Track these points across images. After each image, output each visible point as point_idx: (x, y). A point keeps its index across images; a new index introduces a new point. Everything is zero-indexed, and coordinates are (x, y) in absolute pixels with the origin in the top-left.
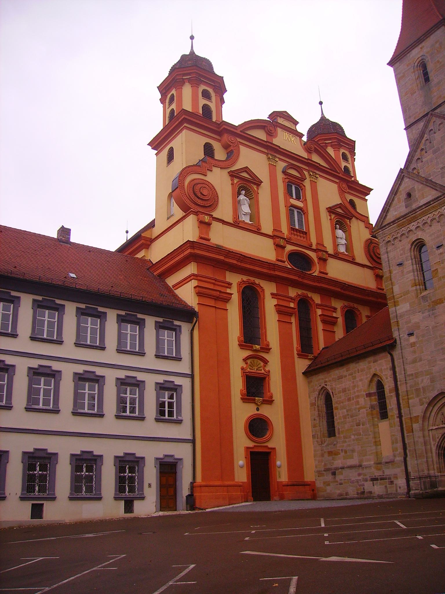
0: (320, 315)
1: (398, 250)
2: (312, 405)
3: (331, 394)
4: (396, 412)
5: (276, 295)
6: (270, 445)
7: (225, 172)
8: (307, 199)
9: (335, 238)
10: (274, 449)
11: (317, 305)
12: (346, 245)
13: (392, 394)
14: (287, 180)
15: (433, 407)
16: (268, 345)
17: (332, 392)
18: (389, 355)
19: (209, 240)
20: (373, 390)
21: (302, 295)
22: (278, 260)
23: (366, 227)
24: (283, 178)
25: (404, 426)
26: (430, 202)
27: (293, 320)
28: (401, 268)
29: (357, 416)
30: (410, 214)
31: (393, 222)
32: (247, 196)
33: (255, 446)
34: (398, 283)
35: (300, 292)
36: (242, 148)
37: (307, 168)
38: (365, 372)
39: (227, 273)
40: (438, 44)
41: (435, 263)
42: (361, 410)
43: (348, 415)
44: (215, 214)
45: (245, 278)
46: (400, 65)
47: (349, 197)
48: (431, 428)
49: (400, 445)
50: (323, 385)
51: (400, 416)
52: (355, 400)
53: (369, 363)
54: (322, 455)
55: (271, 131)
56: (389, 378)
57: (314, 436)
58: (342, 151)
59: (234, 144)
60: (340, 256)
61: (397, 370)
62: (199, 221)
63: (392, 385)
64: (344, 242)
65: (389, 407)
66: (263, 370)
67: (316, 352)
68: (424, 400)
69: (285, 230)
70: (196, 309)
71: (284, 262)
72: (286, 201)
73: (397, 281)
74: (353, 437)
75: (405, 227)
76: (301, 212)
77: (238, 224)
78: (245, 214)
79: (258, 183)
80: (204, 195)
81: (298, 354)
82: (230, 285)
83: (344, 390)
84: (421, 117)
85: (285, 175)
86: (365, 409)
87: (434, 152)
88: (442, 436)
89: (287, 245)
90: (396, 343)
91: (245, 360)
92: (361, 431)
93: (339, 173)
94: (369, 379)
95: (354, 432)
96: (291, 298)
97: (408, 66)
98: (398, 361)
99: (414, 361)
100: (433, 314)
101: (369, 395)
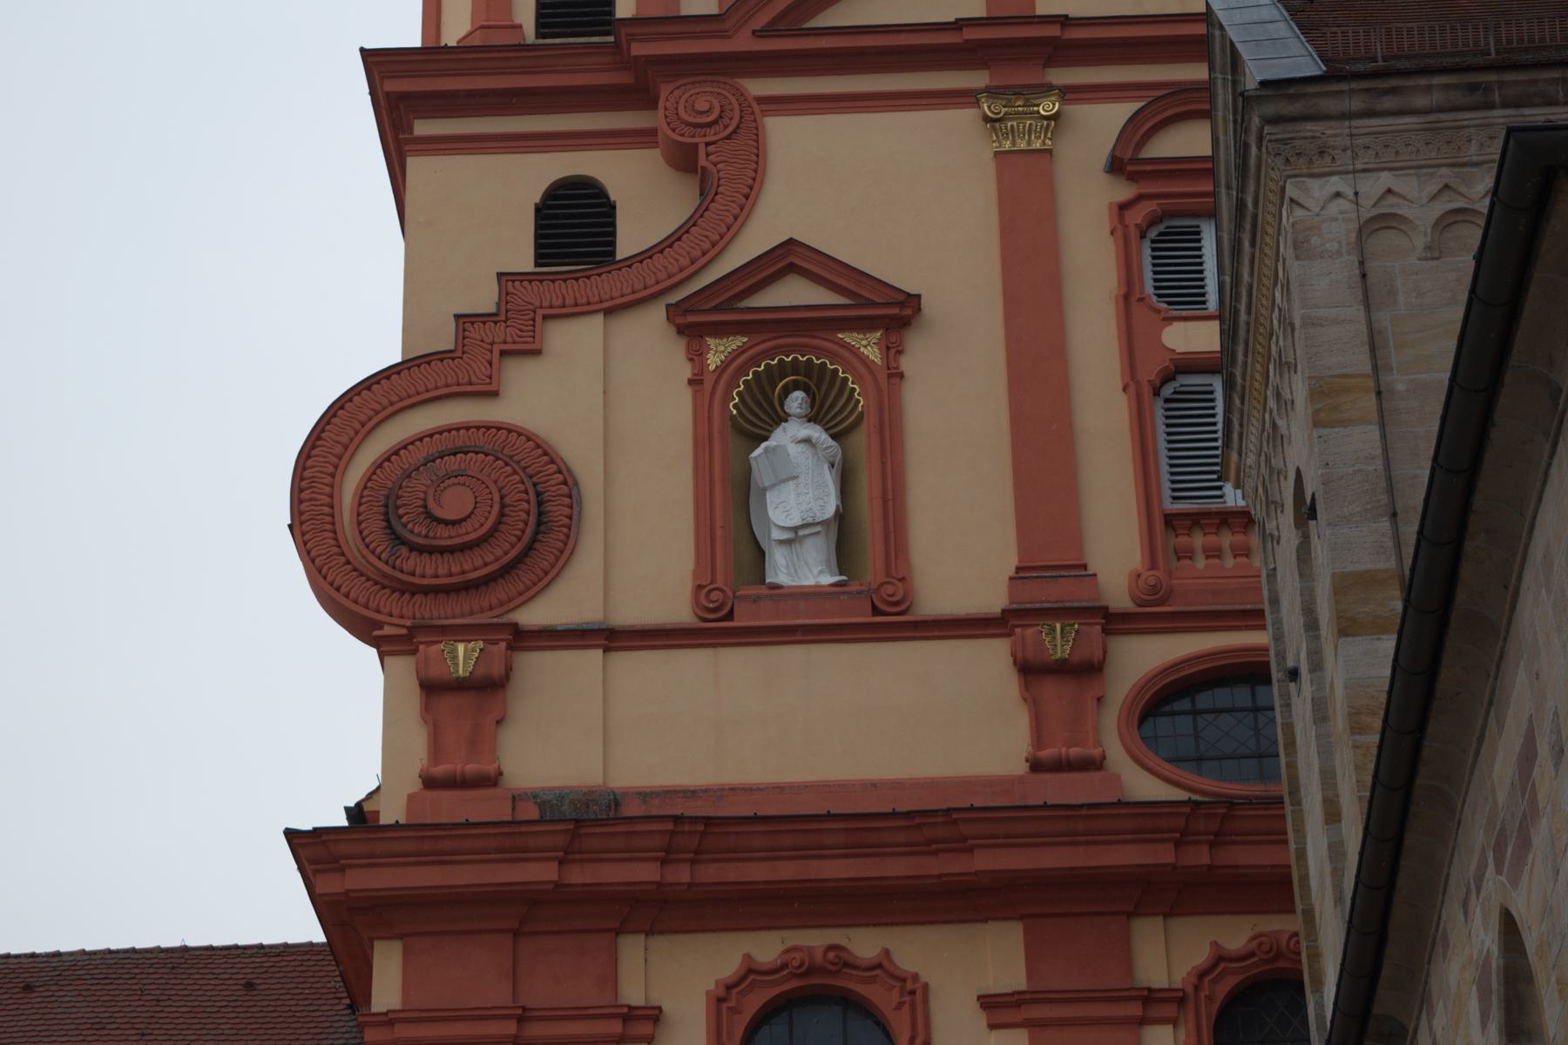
19: (491, 781)
32: (823, 418)
39: (632, 950)
45: (767, 947)
59: (726, 121)
80: (459, 522)
85: (1132, 177)
96: (1150, 997)
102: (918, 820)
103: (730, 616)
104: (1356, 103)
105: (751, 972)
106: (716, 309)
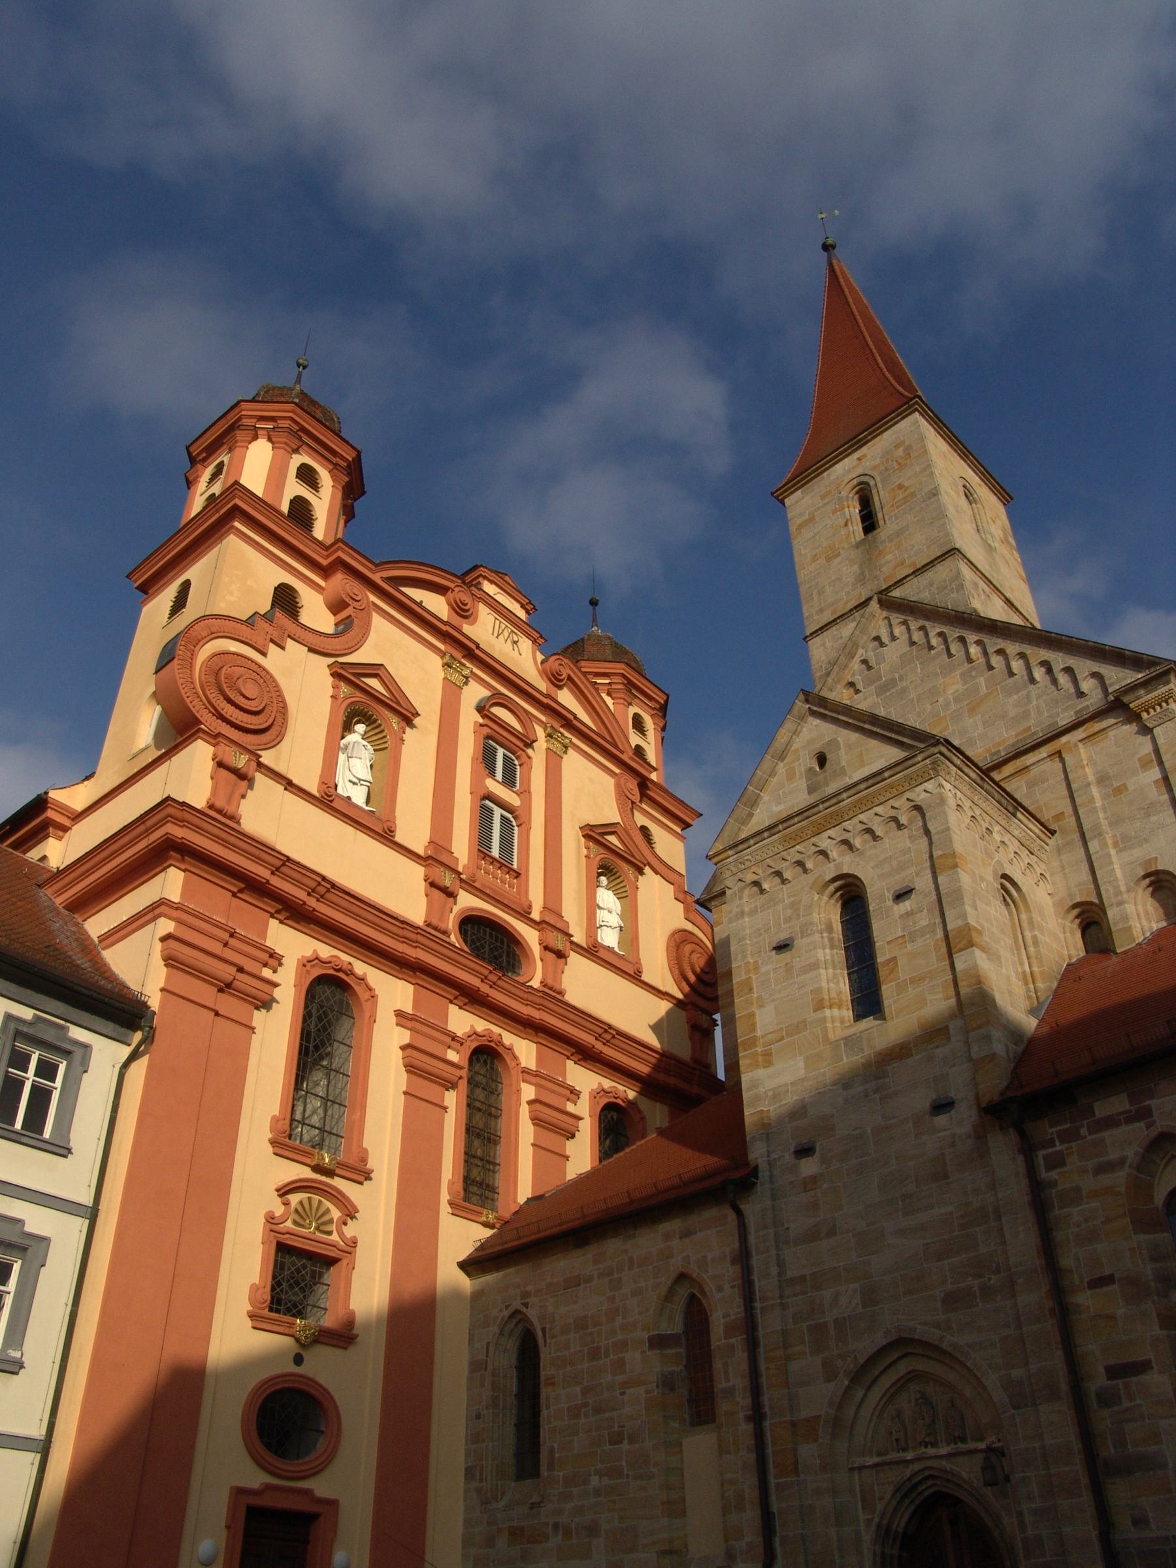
0: (530, 1103)
1: (781, 906)
2: (477, 1366)
3: (539, 1333)
4: (743, 1401)
5: (411, 1020)
6: (321, 1487)
7: (321, 665)
8: (532, 790)
9: (592, 907)
10: (333, 1503)
11: (525, 1071)
12: (621, 930)
13: (733, 1340)
14: (486, 731)
15: (868, 1389)
16: (364, 1160)
17: (544, 1330)
18: (732, 1216)
20: (674, 1325)
21: (484, 1036)
22: (428, 925)
23: (676, 899)
24: (476, 722)
25: (769, 1451)
26: (883, 772)
27: (451, 1099)
28: (785, 956)
29: (614, 1409)
30: (821, 807)
31: (771, 829)
33: (268, 1487)
34: (773, 1000)
35: (481, 1025)
36: (377, 620)
37: (543, 718)
38: (650, 1267)
40: (902, 449)
41: (889, 943)
42: (628, 1391)
43: (586, 1405)
44: (267, 758)
45: (326, 951)
46: (803, 498)
47: (640, 820)
48: (859, 1461)
49: (751, 1516)
50: (517, 1304)
51: (757, 1415)
52: (612, 1357)
53: (667, 1237)
54: (490, 1542)
55: (465, 605)
56: (727, 1286)
57: (469, 1473)
58: (633, 710)
60: (602, 954)
61: (756, 1261)
62: (217, 760)
63: (736, 1310)
64: (614, 920)
65: (721, 1384)
66: (335, 1233)
67: (506, 1210)
68: (840, 1363)
69: (461, 848)
70: (154, 1001)
71: (445, 933)
72: (476, 782)
73: (771, 995)
74: (595, 1481)
75: (804, 844)
76: (512, 819)
77: (331, 801)
78: (357, 781)
79: (408, 718)
81: (451, 1203)
82: (274, 959)
83: (581, 1324)
84: (851, 610)
86: (641, 1390)
87: (882, 690)
88: (897, 1491)
89: (461, 891)
90: (757, 1179)
91: (285, 1191)
92: (624, 1463)
93: (622, 752)
94: (664, 1290)
95: (600, 1466)
96: (454, 1038)
97: (822, 497)
98: (761, 1233)
99: (812, 1236)
100: (877, 1091)
101: (658, 1342)
102: (405, 926)
103: (331, 801)
104: (958, 762)
105: (316, 959)
106: (353, 674)
